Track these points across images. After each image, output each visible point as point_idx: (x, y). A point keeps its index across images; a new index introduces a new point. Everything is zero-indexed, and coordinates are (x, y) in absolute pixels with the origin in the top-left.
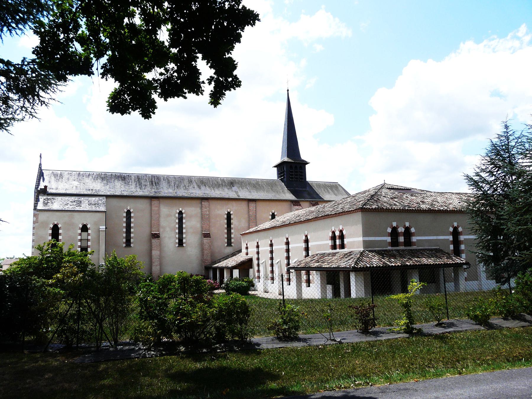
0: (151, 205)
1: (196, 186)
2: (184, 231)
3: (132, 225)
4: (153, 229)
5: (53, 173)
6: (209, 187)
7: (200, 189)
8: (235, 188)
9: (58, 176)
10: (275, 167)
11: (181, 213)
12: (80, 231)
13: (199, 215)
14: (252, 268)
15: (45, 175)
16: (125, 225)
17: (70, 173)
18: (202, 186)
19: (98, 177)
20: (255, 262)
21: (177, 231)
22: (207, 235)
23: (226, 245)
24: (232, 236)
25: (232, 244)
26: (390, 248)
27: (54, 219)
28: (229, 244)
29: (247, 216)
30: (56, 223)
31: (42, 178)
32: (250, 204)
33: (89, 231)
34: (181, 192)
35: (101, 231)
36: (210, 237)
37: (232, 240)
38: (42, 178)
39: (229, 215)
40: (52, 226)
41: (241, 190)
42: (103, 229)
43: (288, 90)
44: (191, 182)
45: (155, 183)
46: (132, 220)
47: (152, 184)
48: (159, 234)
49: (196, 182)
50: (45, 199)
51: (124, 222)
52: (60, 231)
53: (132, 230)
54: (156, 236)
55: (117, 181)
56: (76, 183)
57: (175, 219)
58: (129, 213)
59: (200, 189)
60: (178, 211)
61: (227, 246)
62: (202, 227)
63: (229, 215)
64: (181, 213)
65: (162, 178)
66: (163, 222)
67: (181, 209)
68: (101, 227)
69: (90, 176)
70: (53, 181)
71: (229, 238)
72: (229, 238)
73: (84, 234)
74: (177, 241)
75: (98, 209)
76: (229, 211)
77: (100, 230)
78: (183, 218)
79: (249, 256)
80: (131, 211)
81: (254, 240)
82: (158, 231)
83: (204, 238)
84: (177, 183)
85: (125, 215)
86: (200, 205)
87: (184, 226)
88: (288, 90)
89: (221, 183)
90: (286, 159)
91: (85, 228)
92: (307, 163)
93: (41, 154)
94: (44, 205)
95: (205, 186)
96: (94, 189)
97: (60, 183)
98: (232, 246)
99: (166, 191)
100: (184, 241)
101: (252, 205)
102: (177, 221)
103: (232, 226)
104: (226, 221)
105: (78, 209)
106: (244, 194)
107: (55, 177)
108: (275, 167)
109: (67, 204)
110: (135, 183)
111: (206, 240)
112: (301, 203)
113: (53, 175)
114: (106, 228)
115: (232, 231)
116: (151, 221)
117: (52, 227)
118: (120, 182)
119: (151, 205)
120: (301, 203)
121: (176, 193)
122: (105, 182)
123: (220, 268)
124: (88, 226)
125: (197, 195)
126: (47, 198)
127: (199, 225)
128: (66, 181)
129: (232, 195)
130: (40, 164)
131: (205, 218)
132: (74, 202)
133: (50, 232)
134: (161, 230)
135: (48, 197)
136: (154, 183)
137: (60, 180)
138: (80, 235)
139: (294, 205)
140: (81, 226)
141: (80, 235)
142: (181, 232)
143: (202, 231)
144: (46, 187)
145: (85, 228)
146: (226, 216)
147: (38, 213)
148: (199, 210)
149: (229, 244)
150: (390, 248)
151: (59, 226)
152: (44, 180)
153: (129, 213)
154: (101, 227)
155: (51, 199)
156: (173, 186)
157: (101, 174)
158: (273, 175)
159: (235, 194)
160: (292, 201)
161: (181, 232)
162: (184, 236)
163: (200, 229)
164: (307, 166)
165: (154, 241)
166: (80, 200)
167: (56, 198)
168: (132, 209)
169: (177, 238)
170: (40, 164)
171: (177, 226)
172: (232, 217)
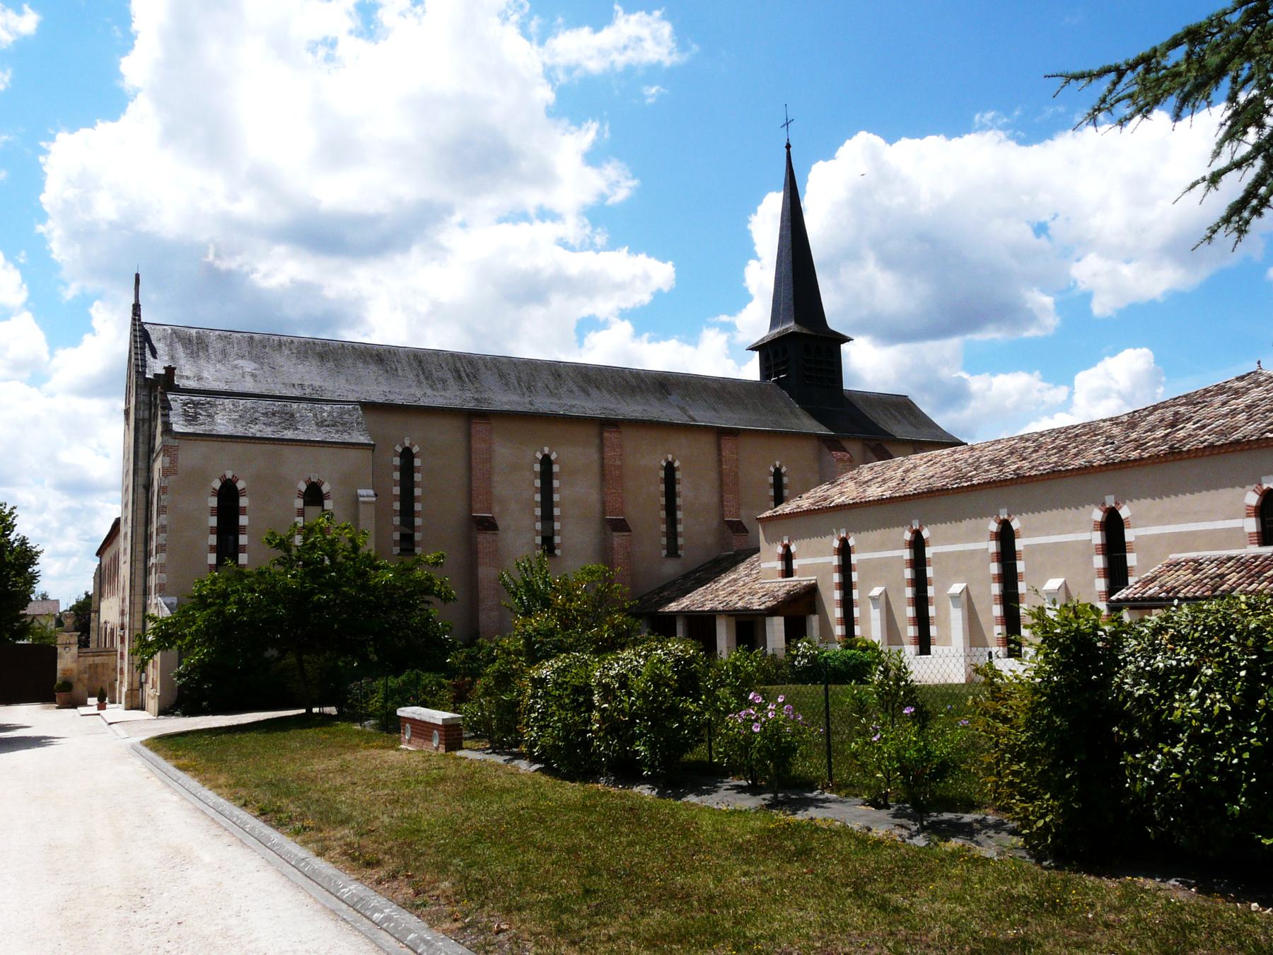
0: (469, 436)
1: (575, 389)
2: (557, 512)
3: (418, 492)
4: (476, 506)
5: (174, 332)
6: (610, 392)
7: (589, 395)
8: (674, 398)
9: (195, 343)
10: (753, 349)
11: (546, 462)
12: (299, 503)
13: (595, 468)
14: (814, 613)
15: (153, 338)
16: (397, 490)
17: (226, 336)
18: (590, 389)
19: (306, 351)
20: (832, 597)
21: (538, 512)
22: (620, 526)
23: (664, 552)
24: (680, 528)
25: (680, 552)
26: (1255, 550)
27: (225, 465)
28: (673, 550)
29: (713, 475)
30: (229, 475)
31: (147, 345)
32: (723, 441)
33: (328, 504)
34: (544, 404)
35: (364, 502)
36: (630, 531)
37: (680, 541)
38: (147, 345)
39: (670, 469)
40: (217, 484)
41: (690, 402)
42: (368, 496)
43: (788, 146)
44: (559, 376)
45: (468, 376)
46: (418, 477)
47: (460, 377)
48: (493, 518)
49: (572, 378)
50: (185, 404)
51: (396, 481)
52: (243, 502)
53: (418, 507)
54: (489, 525)
55: (361, 365)
56: (248, 366)
57: (533, 477)
58: (407, 455)
59: (589, 395)
60: (539, 456)
61: (666, 556)
62: (603, 503)
63: (670, 469)
64: (546, 462)
65: (481, 363)
66: (501, 487)
67: (546, 450)
68: (360, 492)
69: (283, 347)
70: (182, 355)
71: (672, 534)
72: (672, 534)
73: (313, 511)
74: (539, 540)
75: (346, 438)
76: (670, 459)
77: (361, 499)
78: (554, 476)
79: (800, 579)
80: (415, 449)
81: (901, 524)
82: (489, 510)
83: (615, 534)
84: (524, 377)
85: (397, 461)
86: (597, 441)
87: (556, 497)
88: (788, 146)
89: (635, 384)
90: (791, 326)
91: (314, 495)
92: (846, 339)
93: (137, 276)
94: (186, 420)
95: (600, 389)
96: (306, 383)
97: (202, 362)
98: (679, 556)
99: (503, 400)
100: (557, 540)
101: (728, 444)
102: (538, 483)
103: (679, 501)
104: (662, 487)
105: (289, 434)
106: (703, 416)
107: (185, 347)
108: (753, 349)
109: (254, 421)
110: (415, 373)
111: (618, 539)
112: (845, 444)
113: (176, 340)
114: (376, 495)
115: (680, 515)
116: (470, 485)
117: (218, 488)
118: (370, 367)
119: (469, 436)
120: (845, 444)
121: (532, 404)
122: (331, 365)
123: (686, 616)
124: (325, 488)
125: (589, 413)
126: (192, 400)
127: (594, 497)
128: (220, 357)
129: (676, 416)
130: (136, 308)
131: (608, 476)
132: (274, 414)
133: (213, 502)
134: (497, 509)
135: (194, 398)
136: (463, 375)
137: (201, 354)
138: (301, 513)
139: (831, 448)
140: (303, 487)
141: (301, 513)
142: (547, 517)
143: (604, 513)
144: (170, 371)
145: (314, 495)
146: (662, 474)
147: (176, 442)
148: (593, 454)
149: (673, 550)
150: (1255, 550)
151: (240, 485)
152: (154, 353)
153: (407, 455)
154: (360, 492)
155: (203, 404)
156: (516, 384)
157: (314, 343)
158: (751, 370)
159: (679, 411)
160: (820, 438)
161: (547, 517)
162: (557, 526)
163: (597, 508)
164: (845, 347)
165: (483, 539)
166: (288, 409)
167: (219, 401)
168: (416, 446)
169: (537, 531)
170: (136, 308)
171: (538, 497)
172: (678, 475)
